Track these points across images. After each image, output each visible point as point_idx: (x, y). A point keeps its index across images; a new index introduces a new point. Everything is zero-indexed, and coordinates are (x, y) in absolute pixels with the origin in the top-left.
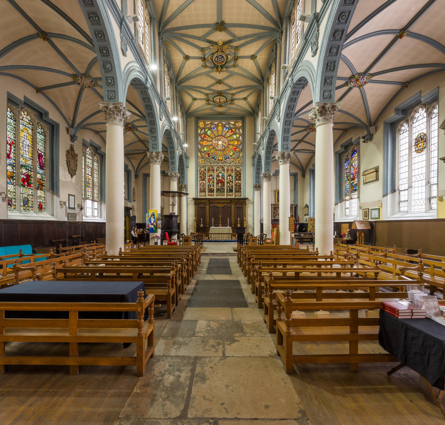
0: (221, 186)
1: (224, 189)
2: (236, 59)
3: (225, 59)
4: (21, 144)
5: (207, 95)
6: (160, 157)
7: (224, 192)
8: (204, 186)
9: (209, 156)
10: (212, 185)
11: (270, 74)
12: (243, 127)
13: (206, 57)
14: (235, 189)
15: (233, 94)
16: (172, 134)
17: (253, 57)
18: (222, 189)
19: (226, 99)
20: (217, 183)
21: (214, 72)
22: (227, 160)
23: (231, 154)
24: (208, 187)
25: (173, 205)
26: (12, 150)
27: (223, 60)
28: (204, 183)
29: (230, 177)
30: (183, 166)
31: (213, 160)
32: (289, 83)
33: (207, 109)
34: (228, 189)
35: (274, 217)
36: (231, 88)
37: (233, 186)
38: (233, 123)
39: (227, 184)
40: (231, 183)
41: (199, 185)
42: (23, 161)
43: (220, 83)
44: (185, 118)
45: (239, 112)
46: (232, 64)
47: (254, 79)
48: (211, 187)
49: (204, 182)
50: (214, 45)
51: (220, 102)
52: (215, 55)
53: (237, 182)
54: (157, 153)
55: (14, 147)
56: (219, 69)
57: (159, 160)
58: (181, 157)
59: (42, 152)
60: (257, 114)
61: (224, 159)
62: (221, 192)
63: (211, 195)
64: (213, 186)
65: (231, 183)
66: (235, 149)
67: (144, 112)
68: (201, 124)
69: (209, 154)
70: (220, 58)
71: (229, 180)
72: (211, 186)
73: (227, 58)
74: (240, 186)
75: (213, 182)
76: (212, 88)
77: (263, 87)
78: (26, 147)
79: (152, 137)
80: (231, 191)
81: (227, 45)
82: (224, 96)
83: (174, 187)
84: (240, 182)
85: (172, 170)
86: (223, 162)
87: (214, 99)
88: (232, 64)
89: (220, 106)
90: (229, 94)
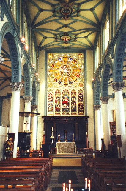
0: (67, 106)
1: (69, 109)
2: (79, 11)
3: (71, 11)
5: (55, 35)
6: (20, 86)
7: (69, 111)
9: (57, 82)
10: (59, 106)
11: (105, 21)
12: (85, 58)
13: (56, 10)
14: (78, 109)
15: (76, 35)
16: (29, 67)
17: (92, 10)
18: (67, 109)
19: (71, 38)
20: (63, 104)
21: (61, 19)
22: (72, 84)
23: (75, 80)
24: (55, 107)
25: (27, 123)
27: (69, 12)
29: (74, 99)
30: (35, 90)
32: (119, 33)
33: (56, 45)
34: (72, 108)
35: (114, 134)
36: (75, 30)
37: (76, 106)
38: (76, 55)
39: (71, 104)
40: (74, 104)
41: (47, 105)
43: (66, 27)
44: (37, 51)
45: (80, 47)
46: (76, 14)
47: (92, 23)
48: (58, 107)
50: (62, 3)
51: (65, 40)
52: (63, 9)
53: (80, 102)
54: (18, 84)
56: (66, 18)
57: (19, 88)
58: (34, 83)
60: (96, 48)
61: (68, 84)
62: (66, 111)
63: (58, 114)
64: (60, 106)
65: (74, 104)
66: (78, 75)
67: (9, 54)
68: (50, 56)
69: (56, 80)
70: (66, 11)
71: (73, 101)
72: (57, 106)
73: (72, 11)
74: (82, 106)
75: (60, 103)
76: (59, 30)
77: (100, 29)
79: (15, 71)
80: (75, 110)
81: (72, 3)
82: (69, 36)
83: (28, 109)
84: (82, 102)
85: (27, 94)
86: (68, 86)
87: (61, 38)
88: (76, 14)
89: (66, 42)
90: (73, 34)
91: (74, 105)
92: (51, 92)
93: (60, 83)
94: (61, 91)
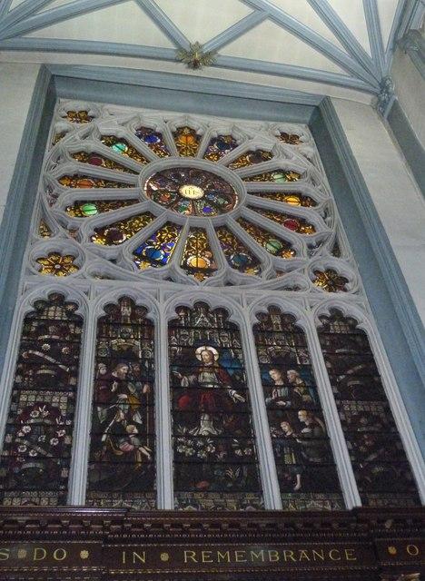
0: (221, 440)
1: (252, 461)
8: (50, 430)
20: (184, 417)
24: (95, 445)
28: (55, 412)
29: (291, 373)
31: (145, 266)
37: (325, 438)
39: (274, 421)
49: (59, 400)
64: (148, 435)
71: (283, 392)
72: (120, 433)
75: (147, 404)
86: (218, 276)
91: (297, 426)
92: (54, 313)
93: (146, 255)
94: (162, 315)
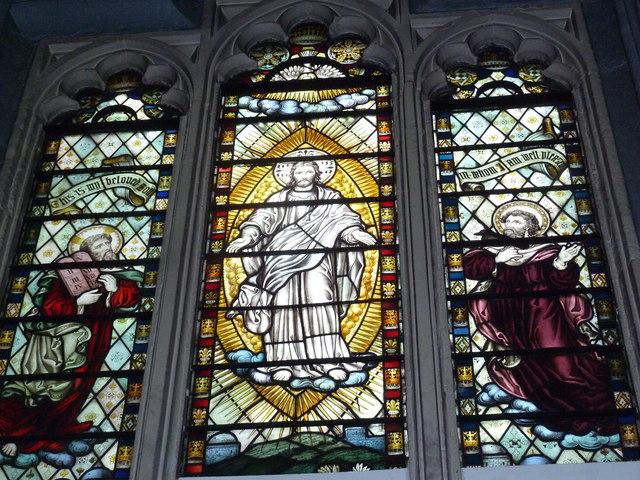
4: (234, 270)
26: (117, 357)
42: (262, 413)
55: (143, 318)
59: (556, 243)
78: (299, 276)
